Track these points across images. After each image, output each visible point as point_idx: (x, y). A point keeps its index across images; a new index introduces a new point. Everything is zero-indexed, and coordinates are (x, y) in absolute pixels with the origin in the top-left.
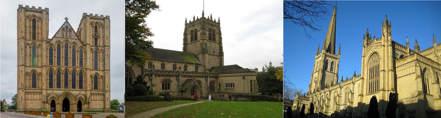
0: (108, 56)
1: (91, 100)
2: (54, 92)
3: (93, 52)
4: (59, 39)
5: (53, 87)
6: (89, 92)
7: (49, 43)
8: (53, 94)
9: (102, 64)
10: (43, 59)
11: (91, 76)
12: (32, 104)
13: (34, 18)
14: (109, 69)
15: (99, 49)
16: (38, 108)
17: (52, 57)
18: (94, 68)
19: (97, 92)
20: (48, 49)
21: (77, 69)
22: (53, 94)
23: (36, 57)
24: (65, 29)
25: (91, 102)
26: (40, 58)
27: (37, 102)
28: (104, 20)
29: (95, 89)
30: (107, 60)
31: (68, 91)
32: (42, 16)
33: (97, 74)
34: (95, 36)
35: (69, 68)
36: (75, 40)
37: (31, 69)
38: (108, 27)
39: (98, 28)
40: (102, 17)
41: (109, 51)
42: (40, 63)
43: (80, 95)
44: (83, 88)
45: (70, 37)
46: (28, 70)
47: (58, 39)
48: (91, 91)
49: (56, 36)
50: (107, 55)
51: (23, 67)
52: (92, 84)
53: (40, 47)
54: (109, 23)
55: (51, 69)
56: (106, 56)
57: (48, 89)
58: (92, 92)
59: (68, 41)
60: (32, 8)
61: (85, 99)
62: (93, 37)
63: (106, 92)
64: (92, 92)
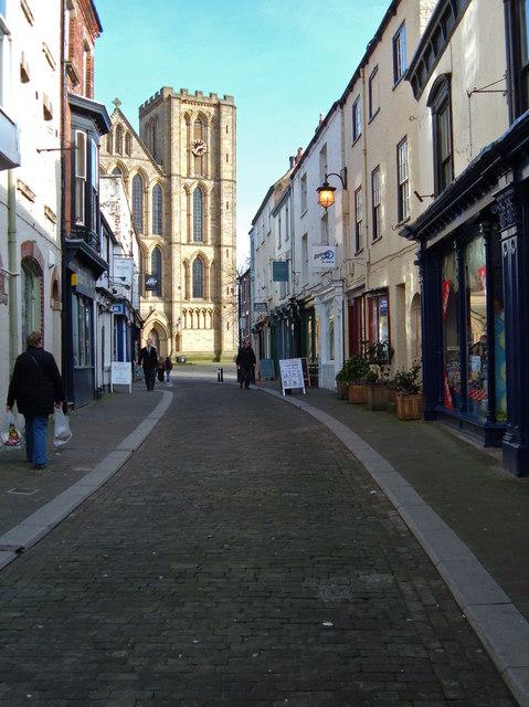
3: (188, 194)
18: (192, 238)
19: (200, 306)
29: (194, 296)
40: (214, 98)
52: (187, 283)
56: (224, 207)
64: (187, 306)
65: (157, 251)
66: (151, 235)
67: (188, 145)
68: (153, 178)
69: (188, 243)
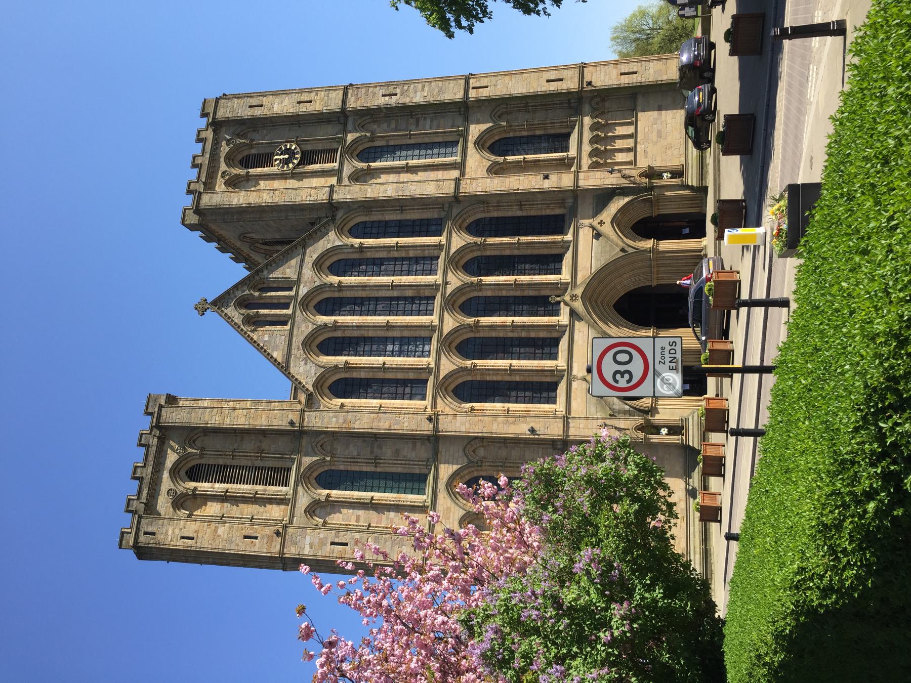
0: (391, 90)
1: (634, 163)
2: (580, 375)
4: (298, 340)
5: (548, 379)
6: (586, 179)
9: (431, 121)
10: (397, 427)
11: (495, 170)
13: (183, 473)
14: (463, 82)
15: (354, 142)
17: (383, 382)
19: (587, 135)
20: (342, 405)
21: (453, 250)
23: (379, 470)
24: (252, 312)
25: (643, 163)
26: (387, 451)
28: (221, 127)
30: (416, 92)
33: (480, 143)
34: (291, 165)
35: (450, 289)
37: (444, 500)
38: (254, 101)
39: (253, 151)
41: (371, 90)
42: (414, 447)
43: (601, 223)
44: (558, 211)
45: (290, 289)
46: (448, 518)
47: (297, 351)
48: (579, 166)
49: (280, 360)
50: (390, 95)
53: (328, 448)
54: (236, 101)
55: (446, 390)
56: (393, 101)
57: (560, 406)
58: (586, 162)
60: (140, 479)
61: (627, 199)
62: (294, 176)
63: (590, 83)
64: (586, 162)
65: (477, 228)
66: (443, 239)
67: (283, 176)
68: (332, 240)
69: (461, 166)
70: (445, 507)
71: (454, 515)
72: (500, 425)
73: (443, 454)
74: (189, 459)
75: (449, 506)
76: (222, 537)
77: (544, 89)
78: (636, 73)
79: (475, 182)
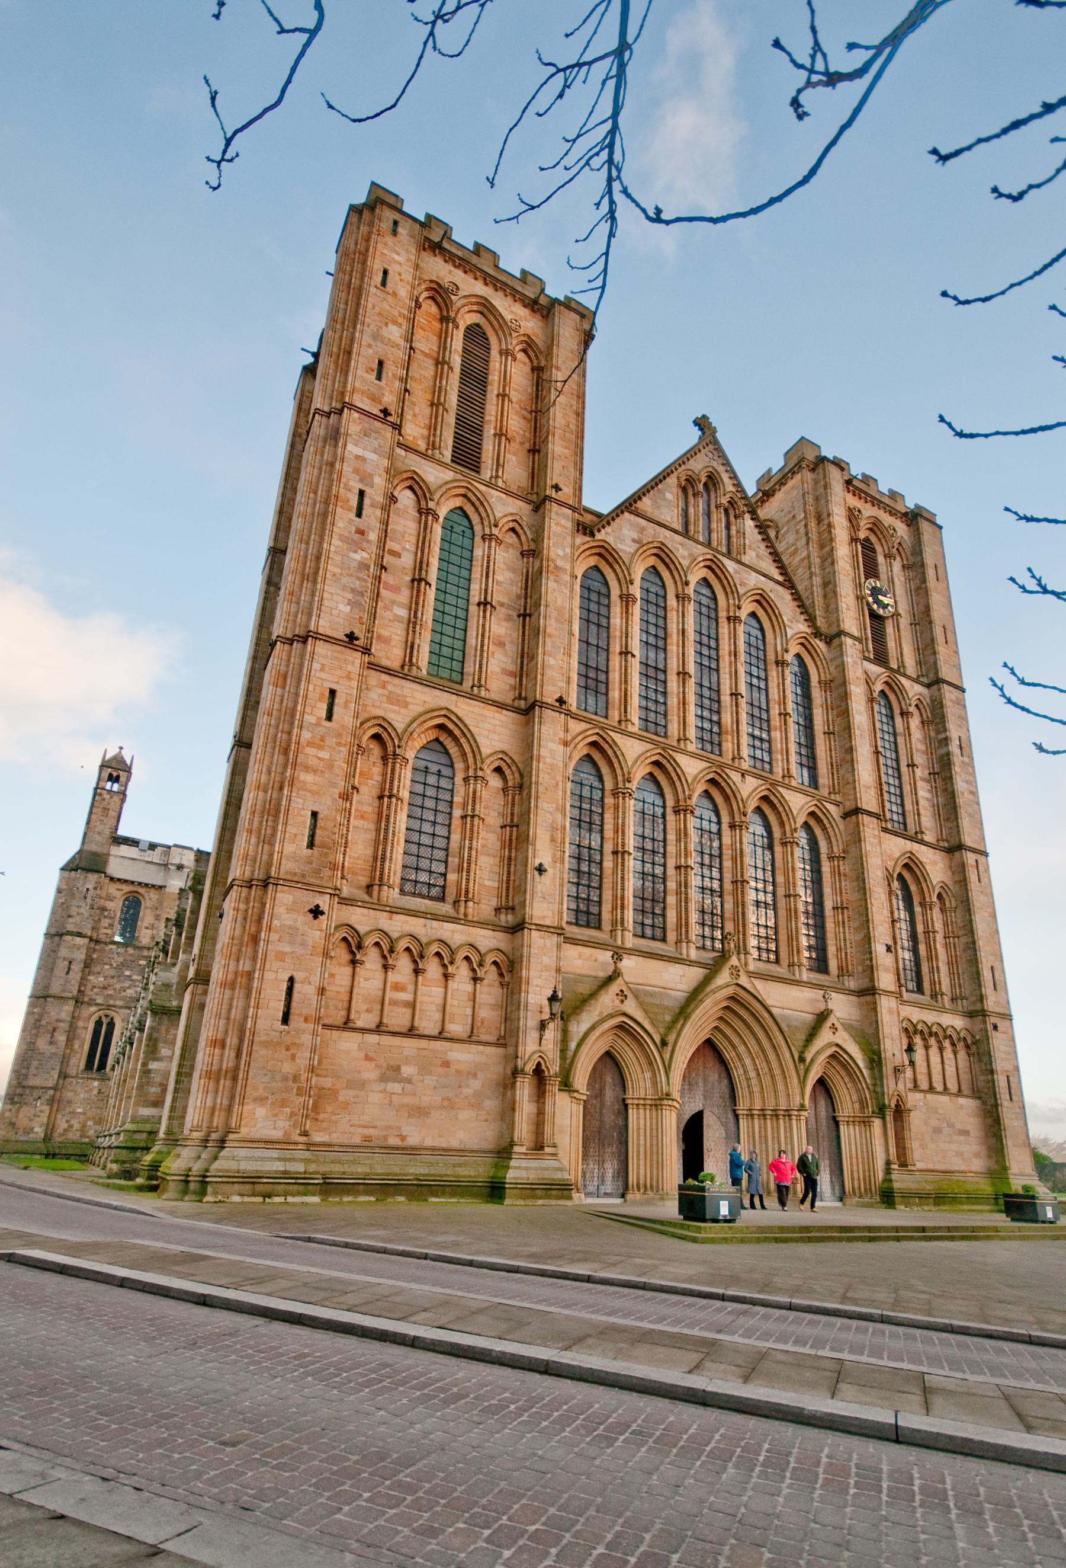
4: (664, 535)
6: (890, 1011)
7: (592, 535)
8: (622, 995)
10: (549, 648)
12: (396, 1087)
16: (455, 1144)
22: (622, 995)
27: (446, 1064)
31: (744, 980)
32: (551, 340)
36: (768, 586)
37: (422, 698)
49: (639, 504)
51: (355, 660)
59: (722, 569)
61: (866, 1072)
70: (409, 700)
71: (394, 711)
72: (549, 816)
73: (498, 715)
74: (500, 333)
75: (411, 707)
76: (384, 328)
77: (984, 960)
78: (1011, 1099)
79: (876, 841)
